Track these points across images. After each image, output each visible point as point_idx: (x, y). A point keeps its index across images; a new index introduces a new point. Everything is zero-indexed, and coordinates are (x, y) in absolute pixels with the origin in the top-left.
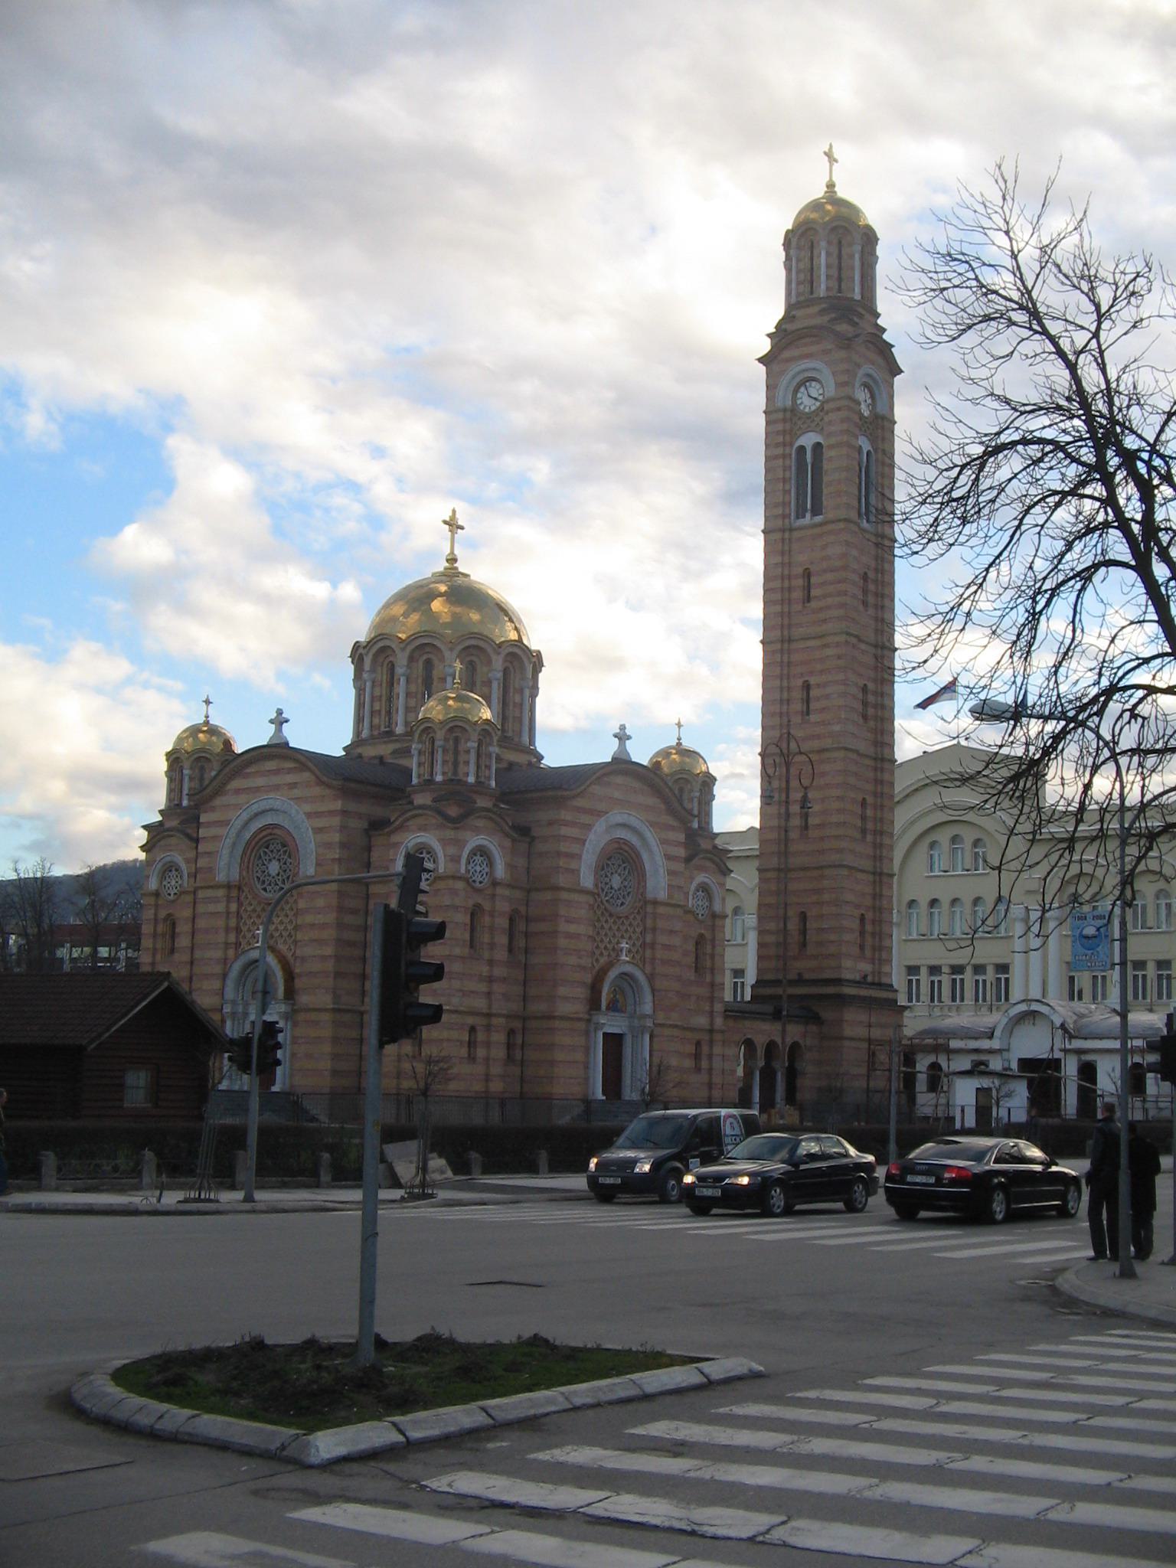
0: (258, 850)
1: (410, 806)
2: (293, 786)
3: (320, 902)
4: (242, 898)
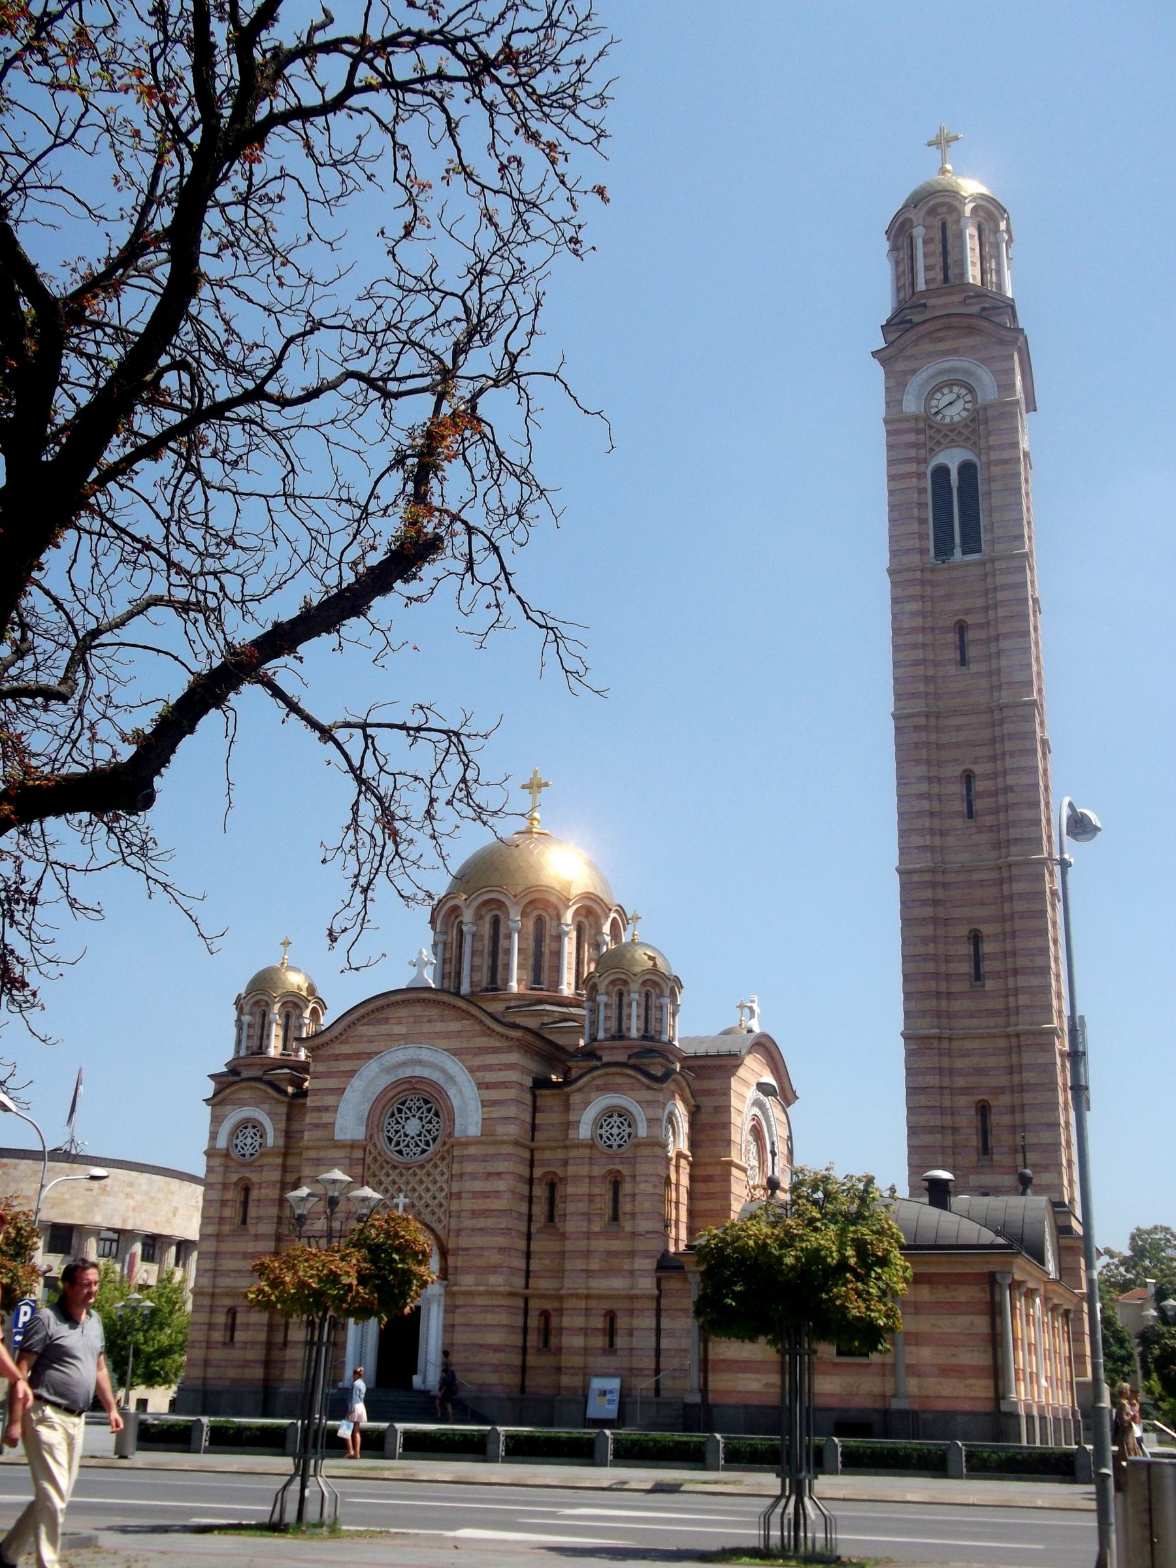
1: (599, 1063)
4: (369, 1160)
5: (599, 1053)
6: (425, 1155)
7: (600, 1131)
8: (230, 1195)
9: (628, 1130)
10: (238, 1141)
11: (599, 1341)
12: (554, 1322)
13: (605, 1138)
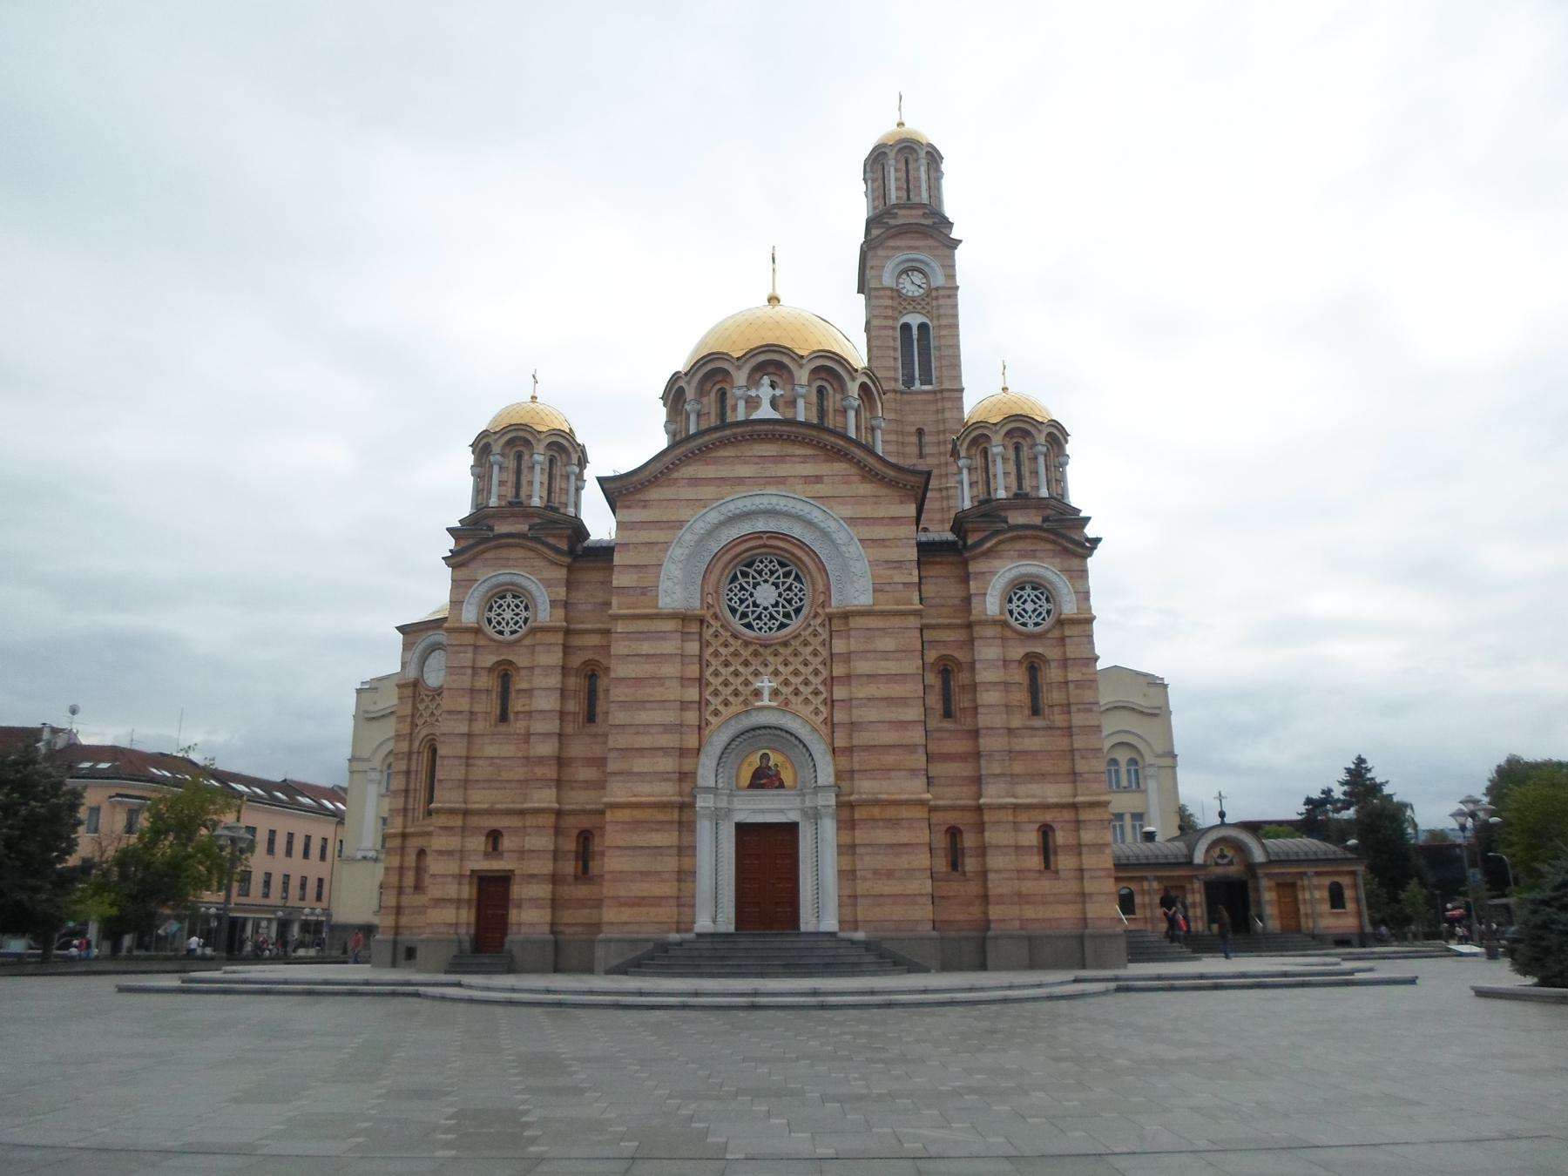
0: (735, 567)
2: (818, 479)
3: (887, 643)
4: (708, 634)
5: (1003, 514)
6: (784, 631)
8: (484, 681)
9: (1046, 606)
10: (492, 615)
11: (1035, 861)
12: (969, 840)
13: (1016, 614)
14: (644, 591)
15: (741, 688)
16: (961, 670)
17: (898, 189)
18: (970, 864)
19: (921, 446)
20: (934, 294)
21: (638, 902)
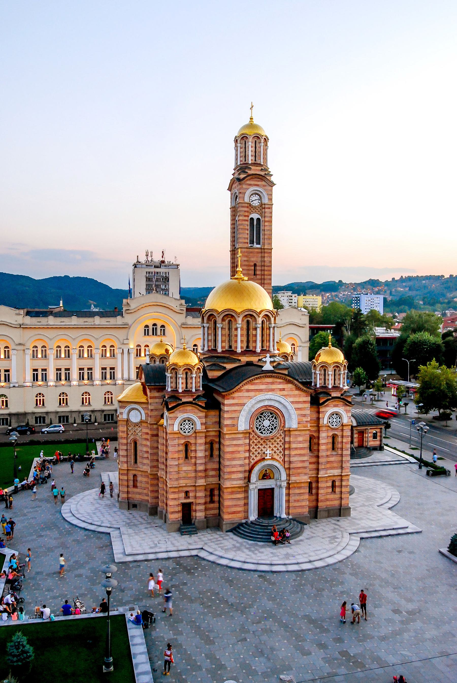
2: (284, 390)
3: (301, 439)
4: (251, 436)
7: (329, 420)
9: (339, 420)
10: (182, 427)
11: (330, 490)
12: (314, 485)
14: (234, 425)
15: (260, 452)
16: (315, 438)
17: (252, 156)
18: (314, 491)
19: (255, 270)
20: (263, 206)
21: (234, 513)
